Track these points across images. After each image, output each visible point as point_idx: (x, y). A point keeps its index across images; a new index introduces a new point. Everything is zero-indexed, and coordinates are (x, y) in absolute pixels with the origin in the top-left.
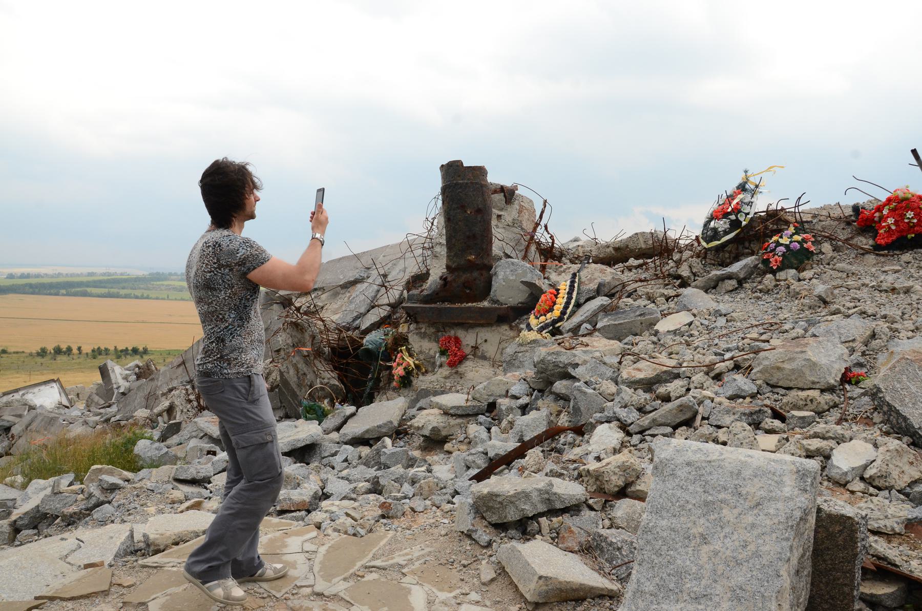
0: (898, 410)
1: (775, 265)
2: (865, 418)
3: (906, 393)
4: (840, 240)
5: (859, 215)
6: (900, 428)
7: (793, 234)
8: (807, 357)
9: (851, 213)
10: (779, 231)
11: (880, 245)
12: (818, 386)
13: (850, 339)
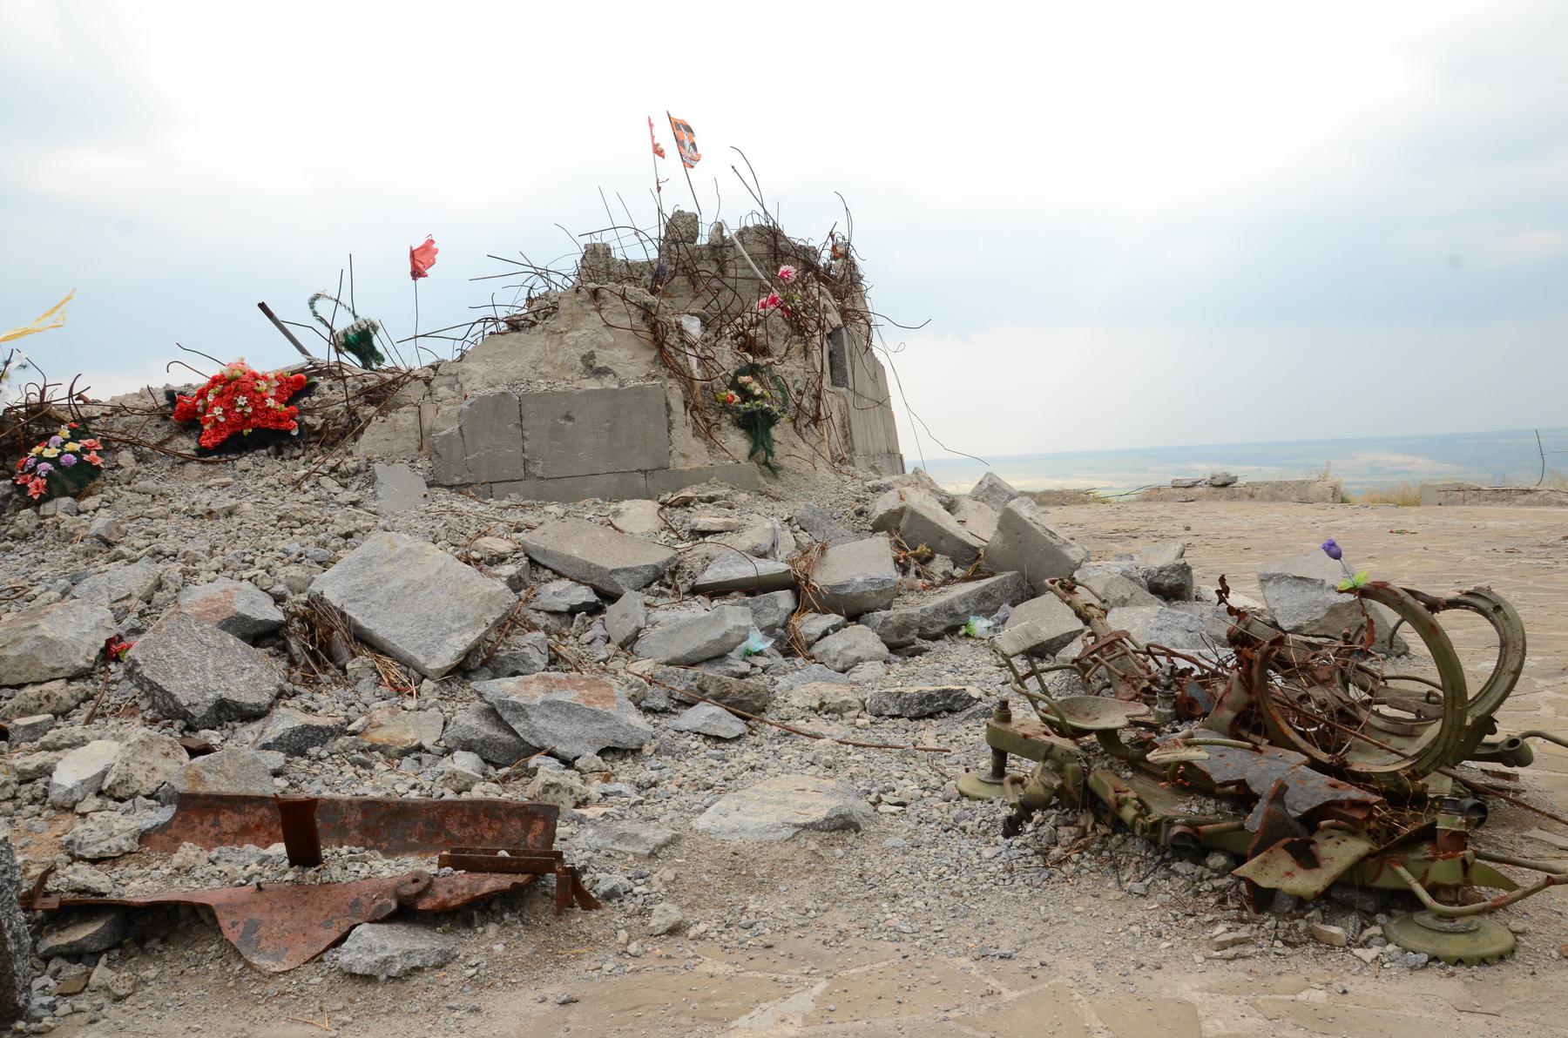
0: (161, 687)
1: (35, 494)
2: (132, 707)
3: (173, 661)
4: (148, 444)
5: (176, 403)
6: (169, 710)
7: (67, 441)
8: (40, 634)
9: (166, 402)
10: (44, 438)
11: (206, 448)
12: (61, 674)
13: (124, 595)
